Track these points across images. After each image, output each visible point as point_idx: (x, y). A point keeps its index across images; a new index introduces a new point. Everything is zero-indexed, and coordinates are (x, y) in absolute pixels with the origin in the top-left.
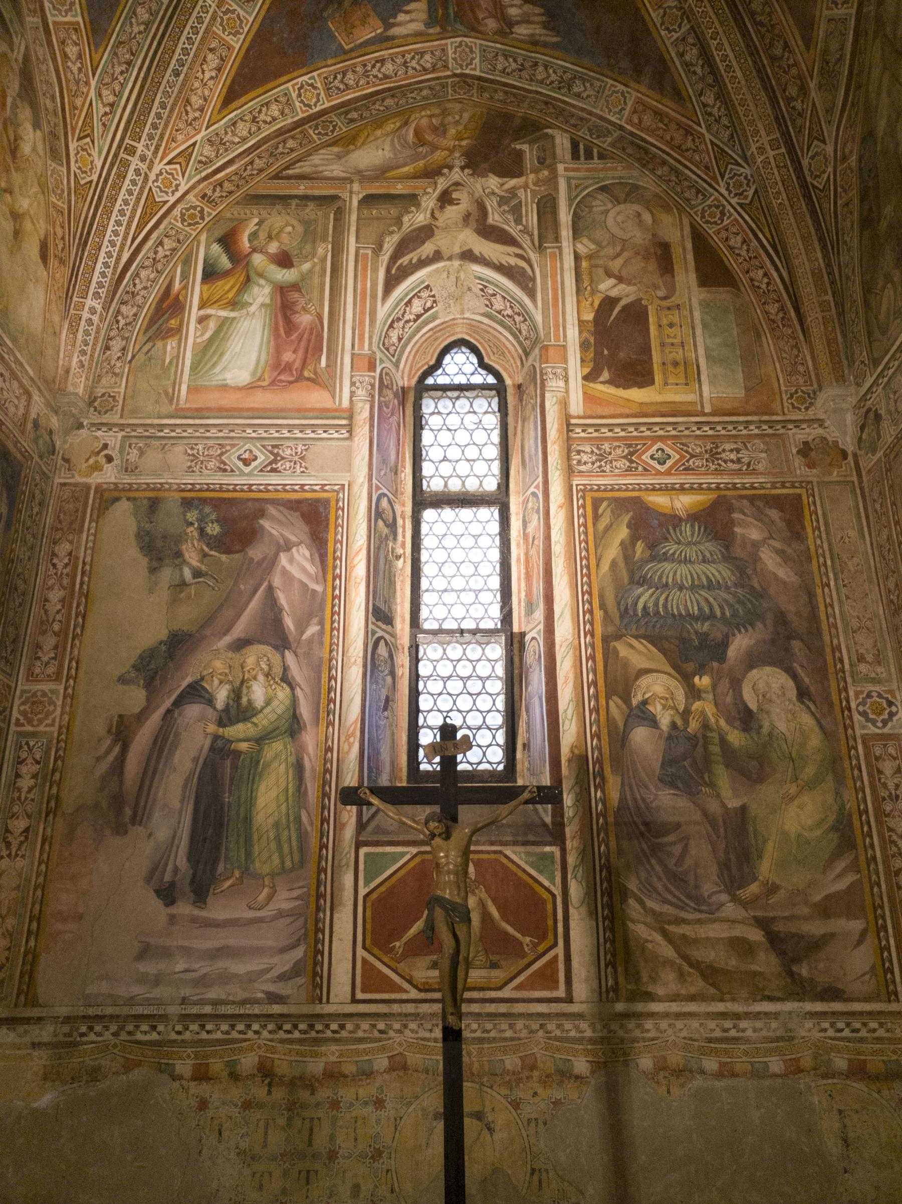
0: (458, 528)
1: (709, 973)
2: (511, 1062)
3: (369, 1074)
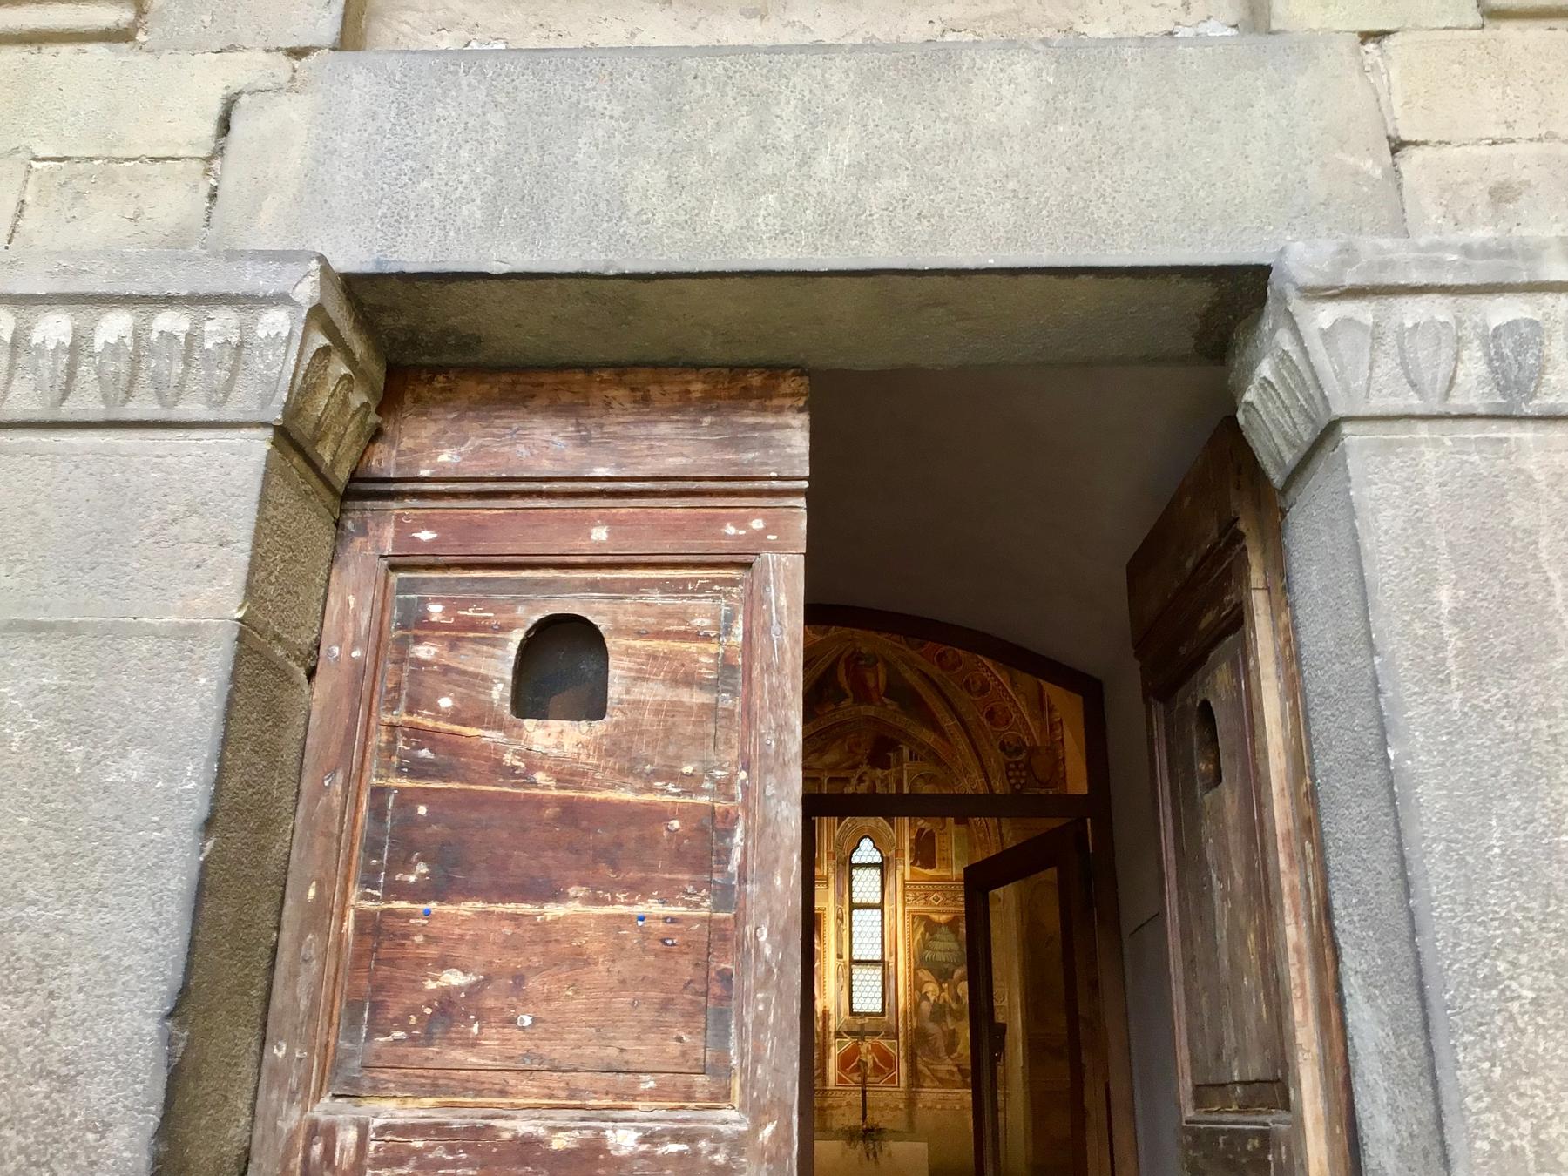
0: (865, 918)
1: (941, 1080)
2: (882, 1105)
3: (840, 1107)
